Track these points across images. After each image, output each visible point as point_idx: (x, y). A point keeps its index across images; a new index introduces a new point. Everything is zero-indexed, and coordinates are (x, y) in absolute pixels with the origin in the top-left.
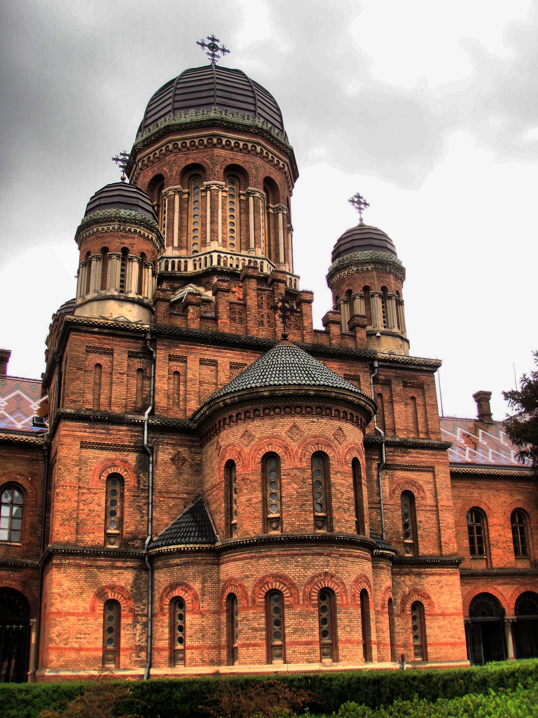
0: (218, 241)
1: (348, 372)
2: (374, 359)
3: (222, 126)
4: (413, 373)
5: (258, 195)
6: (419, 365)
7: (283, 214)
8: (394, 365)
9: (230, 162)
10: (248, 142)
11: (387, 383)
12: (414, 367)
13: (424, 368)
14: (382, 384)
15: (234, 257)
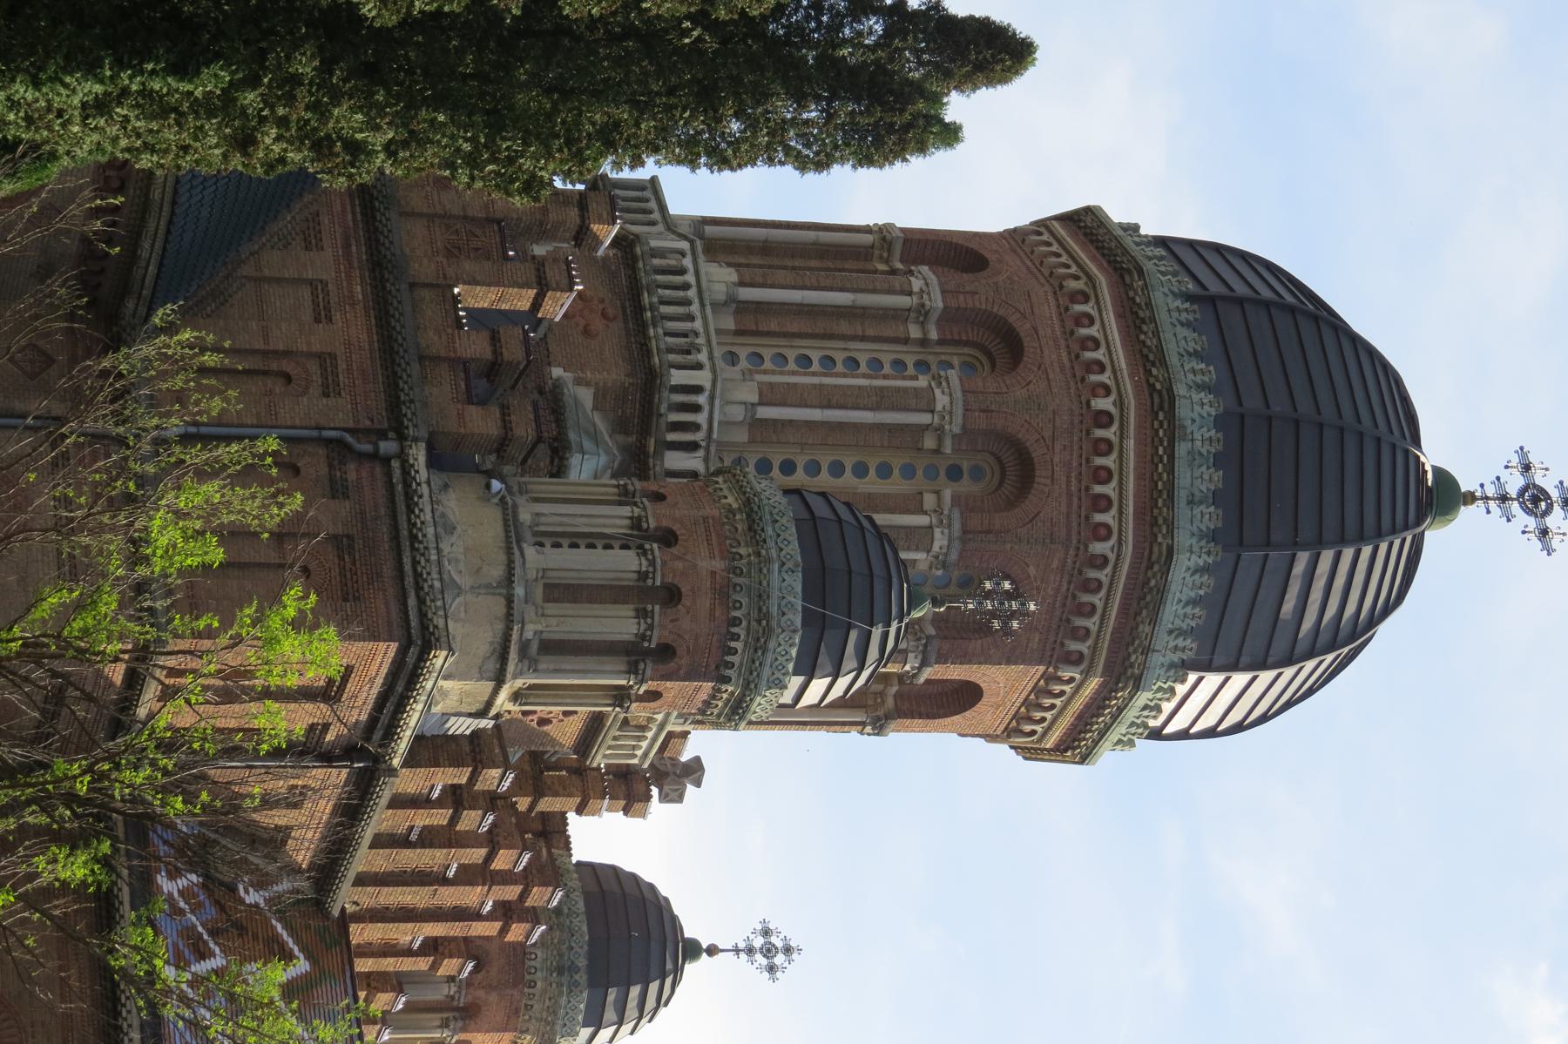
0: (742, 284)
1: (342, 366)
2: (402, 437)
3: (1131, 294)
4: (388, 570)
5: (942, 400)
6: (417, 575)
7: (931, 527)
8: (401, 507)
9: (1023, 328)
10: (1114, 372)
11: (337, 490)
12: (408, 568)
13: (412, 602)
14: (332, 480)
15: (692, 293)
